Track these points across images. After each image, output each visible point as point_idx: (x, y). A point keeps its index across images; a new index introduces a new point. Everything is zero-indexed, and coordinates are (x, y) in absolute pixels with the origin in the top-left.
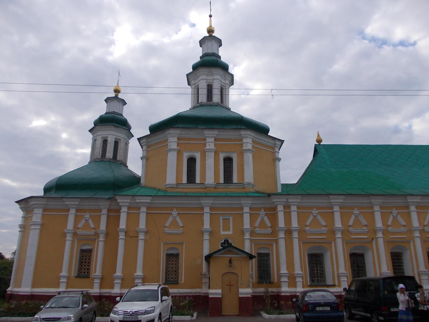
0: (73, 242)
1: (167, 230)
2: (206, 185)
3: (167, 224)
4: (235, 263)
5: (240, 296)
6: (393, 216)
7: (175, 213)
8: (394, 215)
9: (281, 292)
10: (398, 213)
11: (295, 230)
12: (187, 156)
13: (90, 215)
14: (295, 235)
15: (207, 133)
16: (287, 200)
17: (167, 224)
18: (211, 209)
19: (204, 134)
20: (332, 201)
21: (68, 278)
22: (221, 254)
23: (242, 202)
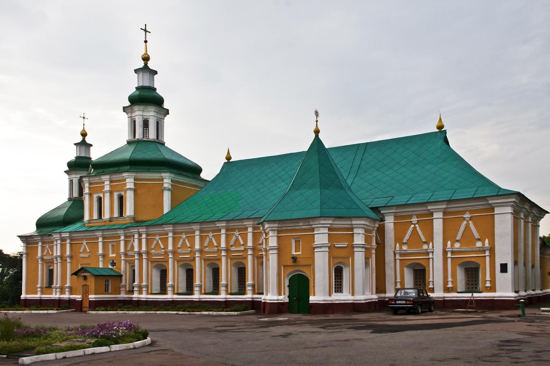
0: (42, 264)
1: (82, 255)
2: (104, 220)
3: (81, 251)
4: (89, 278)
5: (90, 300)
6: (210, 238)
7: (85, 242)
8: (210, 237)
9: (132, 298)
10: (213, 236)
11: (144, 253)
12: (96, 197)
13: (49, 246)
14: (144, 256)
15: (106, 178)
16: (138, 230)
17: (81, 251)
18: (104, 238)
19: (102, 179)
20: (165, 229)
21: (41, 288)
22: (81, 273)
23: (118, 232)
